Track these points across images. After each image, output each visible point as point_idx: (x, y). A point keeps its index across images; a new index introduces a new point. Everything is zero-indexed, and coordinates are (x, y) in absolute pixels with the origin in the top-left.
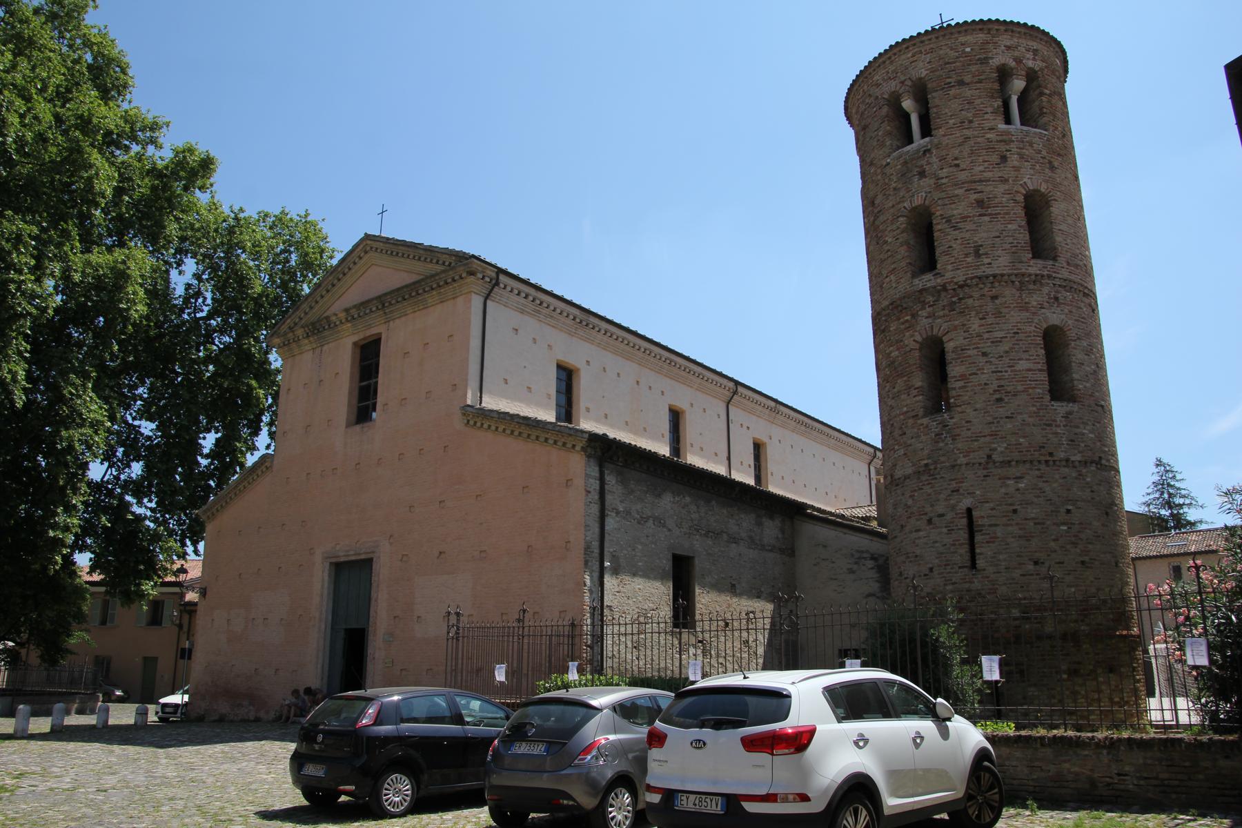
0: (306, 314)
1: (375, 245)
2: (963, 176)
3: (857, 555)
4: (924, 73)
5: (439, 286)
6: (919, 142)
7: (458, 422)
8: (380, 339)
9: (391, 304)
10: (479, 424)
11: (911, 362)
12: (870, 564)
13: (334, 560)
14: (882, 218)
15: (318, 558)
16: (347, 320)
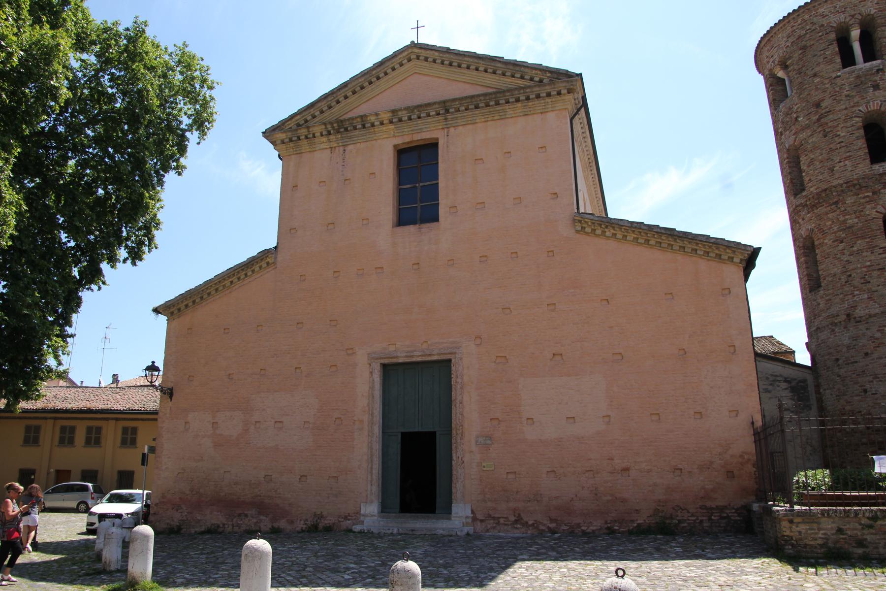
0: (322, 112)
1: (423, 53)
3: (771, 378)
5: (528, 99)
6: (861, 64)
7: (566, 230)
8: (437, 144)
9: (458, 110)
10: (599, 232)
11: (874, 227)
12: (784, 385)
13: (386, 361)
14: (831, 117)
15: (361, 357)
16: (391, 122)
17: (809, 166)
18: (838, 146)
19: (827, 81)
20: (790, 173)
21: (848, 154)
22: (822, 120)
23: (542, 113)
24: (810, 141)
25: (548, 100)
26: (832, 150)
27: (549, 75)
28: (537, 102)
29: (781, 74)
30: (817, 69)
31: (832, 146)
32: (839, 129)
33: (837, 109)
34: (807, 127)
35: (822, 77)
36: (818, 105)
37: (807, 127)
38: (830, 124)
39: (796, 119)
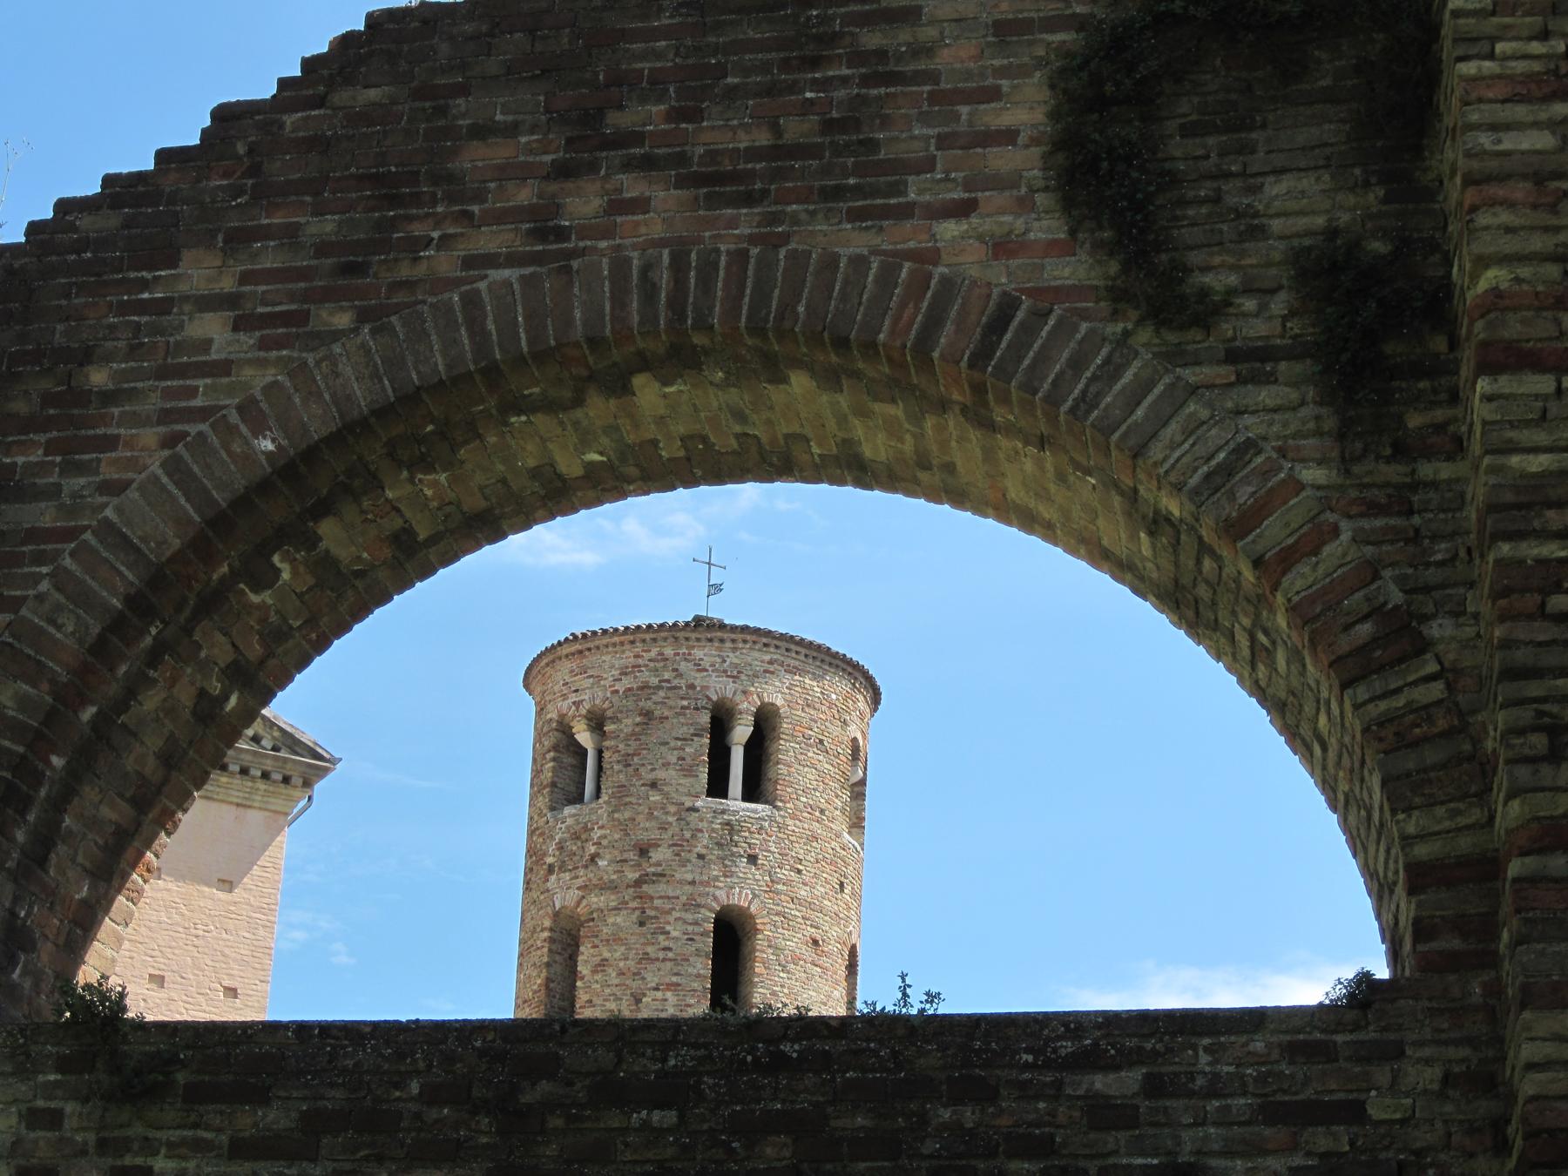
2: (803, 892)
4: (779, 702)
17: (594, 972)
18: (661, 955)
19: (672, 809)
20: (548, 965)
21: (674, 979)
22: (645, 887)
23: (238, 805)
24: (610, 920)
25: (261, 785)
26: (646, 958)
27: (276, 734)
28: (237, 781)
29: (584, 738)
30: (661, 774)
31: (649, 949)
32: (671, 919)
33: (678, 876)
34: (612, 887)
35: (666, 795)
36: (643, 852)
37: (612, 887)
38: (657, 902)
39: (593, 858)
